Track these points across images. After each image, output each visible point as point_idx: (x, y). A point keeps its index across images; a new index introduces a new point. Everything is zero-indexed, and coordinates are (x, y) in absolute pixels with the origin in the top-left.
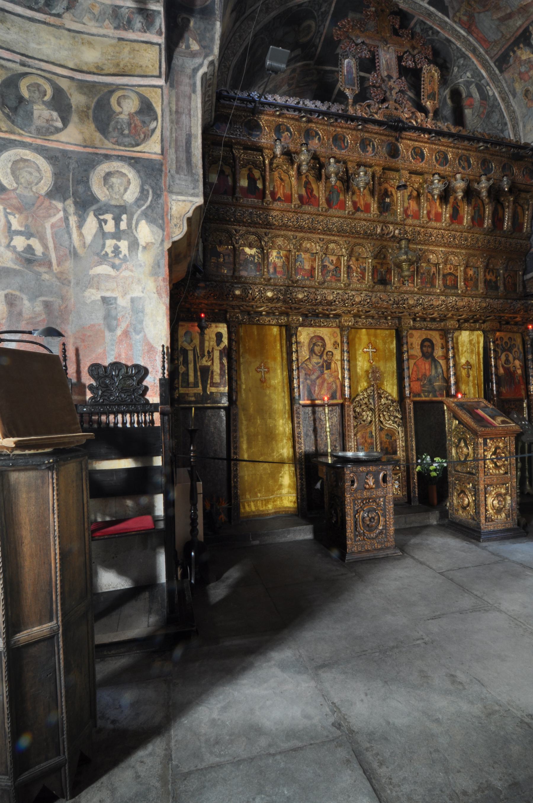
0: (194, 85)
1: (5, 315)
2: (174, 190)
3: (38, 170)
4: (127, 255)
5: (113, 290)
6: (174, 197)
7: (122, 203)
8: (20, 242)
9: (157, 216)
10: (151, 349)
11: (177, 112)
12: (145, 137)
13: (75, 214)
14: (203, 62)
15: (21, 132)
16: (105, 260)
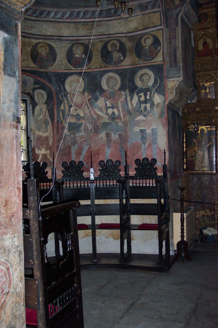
0: (177, 22)
1: (106, 141)
2: (170, 76)
3: (116, 80)
4: (150, 110)
5: (145, 126)
6: (169, 80)
7: (147, 87)
8: (110, 111)
9: (161, 90)
10: (160, 150)
11: (170, 39)
12: (156, 55)
13: (130, 95)
14: (181, 8)
15: (109, 66)
16: (141, 114)
